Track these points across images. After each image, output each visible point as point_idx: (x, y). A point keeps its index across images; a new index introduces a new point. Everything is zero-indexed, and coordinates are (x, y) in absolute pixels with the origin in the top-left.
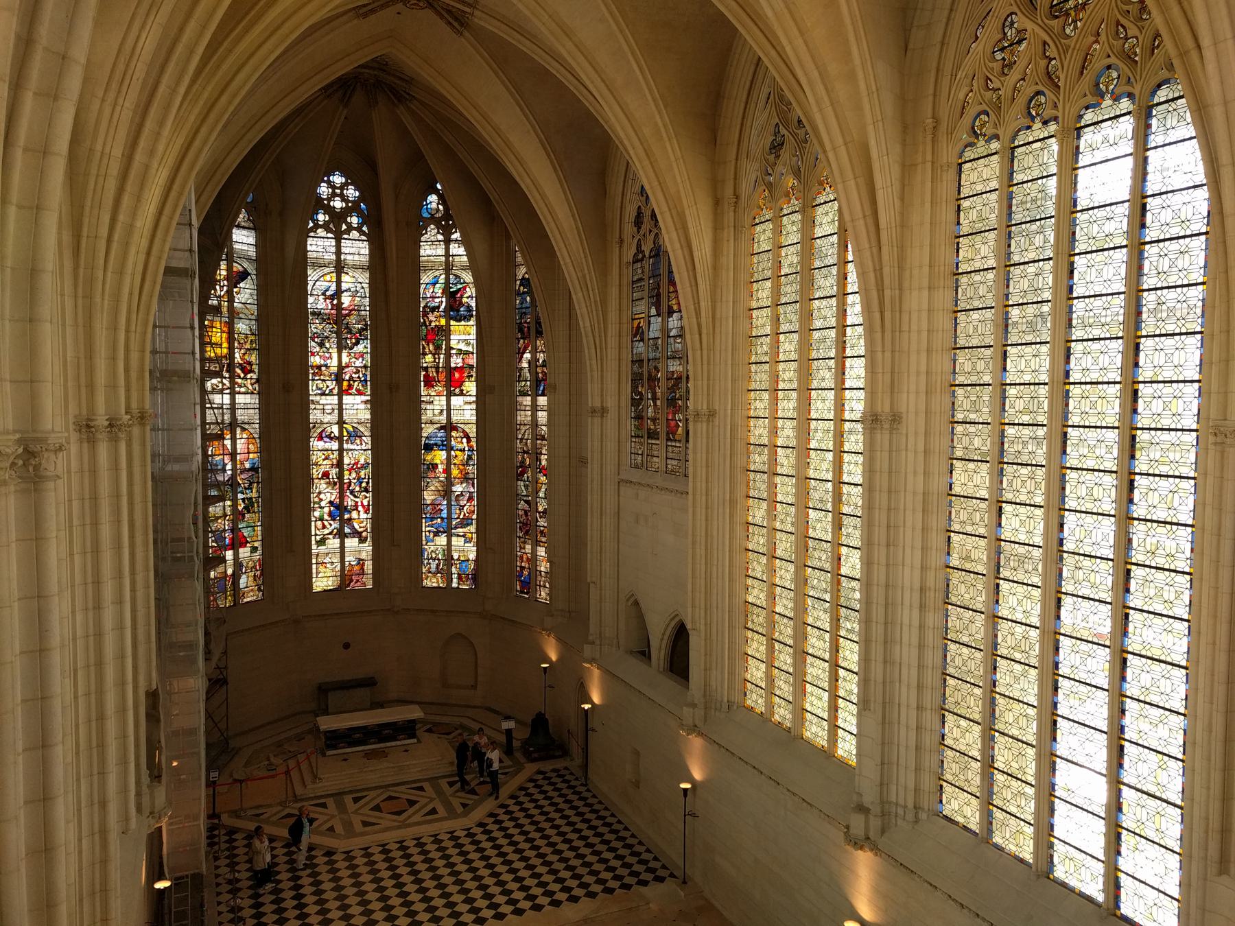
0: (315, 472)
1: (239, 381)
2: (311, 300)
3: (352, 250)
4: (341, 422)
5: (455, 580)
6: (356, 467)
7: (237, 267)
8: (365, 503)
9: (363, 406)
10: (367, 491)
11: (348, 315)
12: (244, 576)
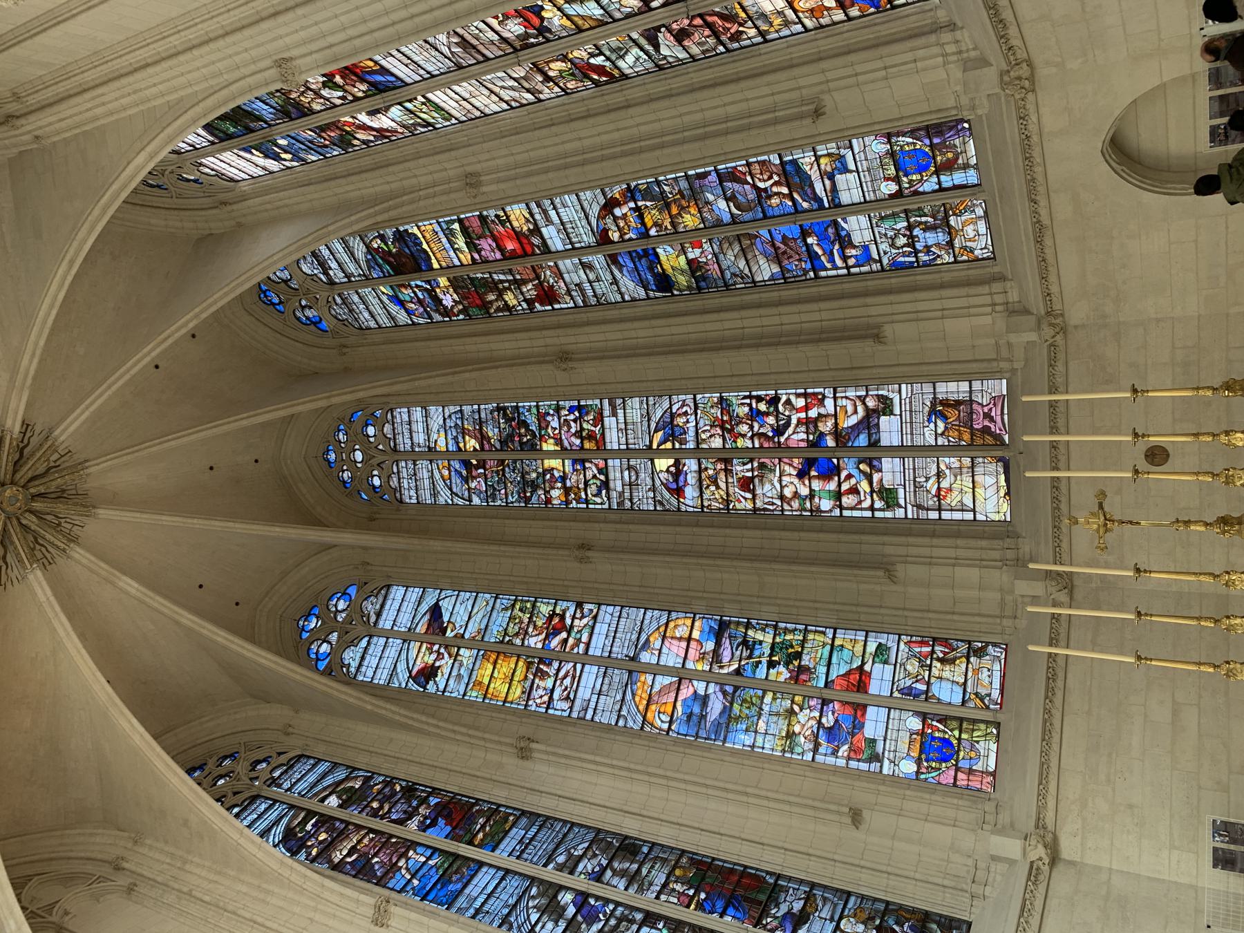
0: (744, 503)
1: (571, 641)
3: (407, 435)
4: (650, 453)
5: (959, 178)
6: (727, 426)
7: (421, 629)
8: (801, 403)
9: (620, 412)
10: (774, 401)
11: (489, 439)
12: (935, 690)
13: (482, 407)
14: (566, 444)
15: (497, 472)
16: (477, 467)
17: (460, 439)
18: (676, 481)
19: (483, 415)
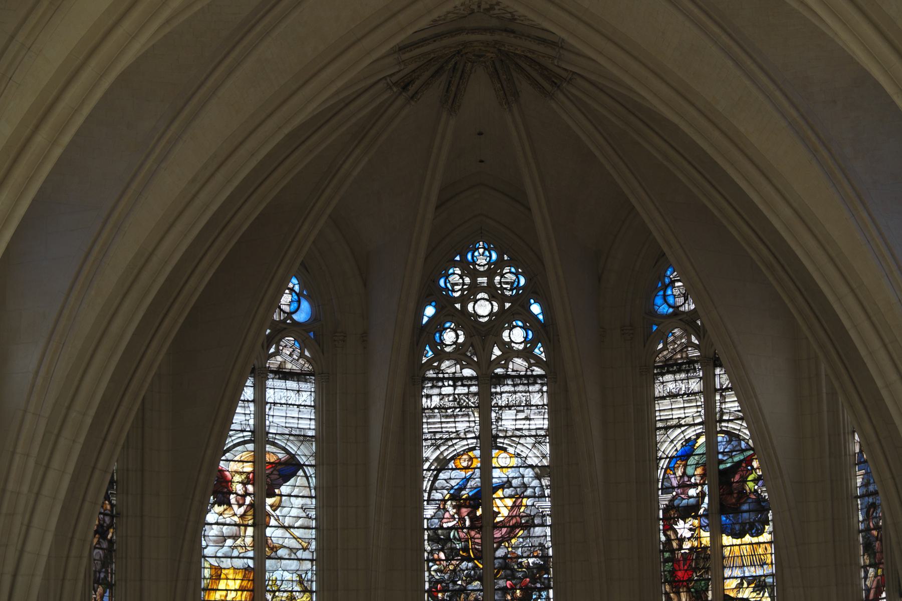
2: (429, 511)
3: (513, 399)
7: (273, 454)
11: (507, 538)
16: (473, 518)
17: (508, 491)
19: (538, 531)
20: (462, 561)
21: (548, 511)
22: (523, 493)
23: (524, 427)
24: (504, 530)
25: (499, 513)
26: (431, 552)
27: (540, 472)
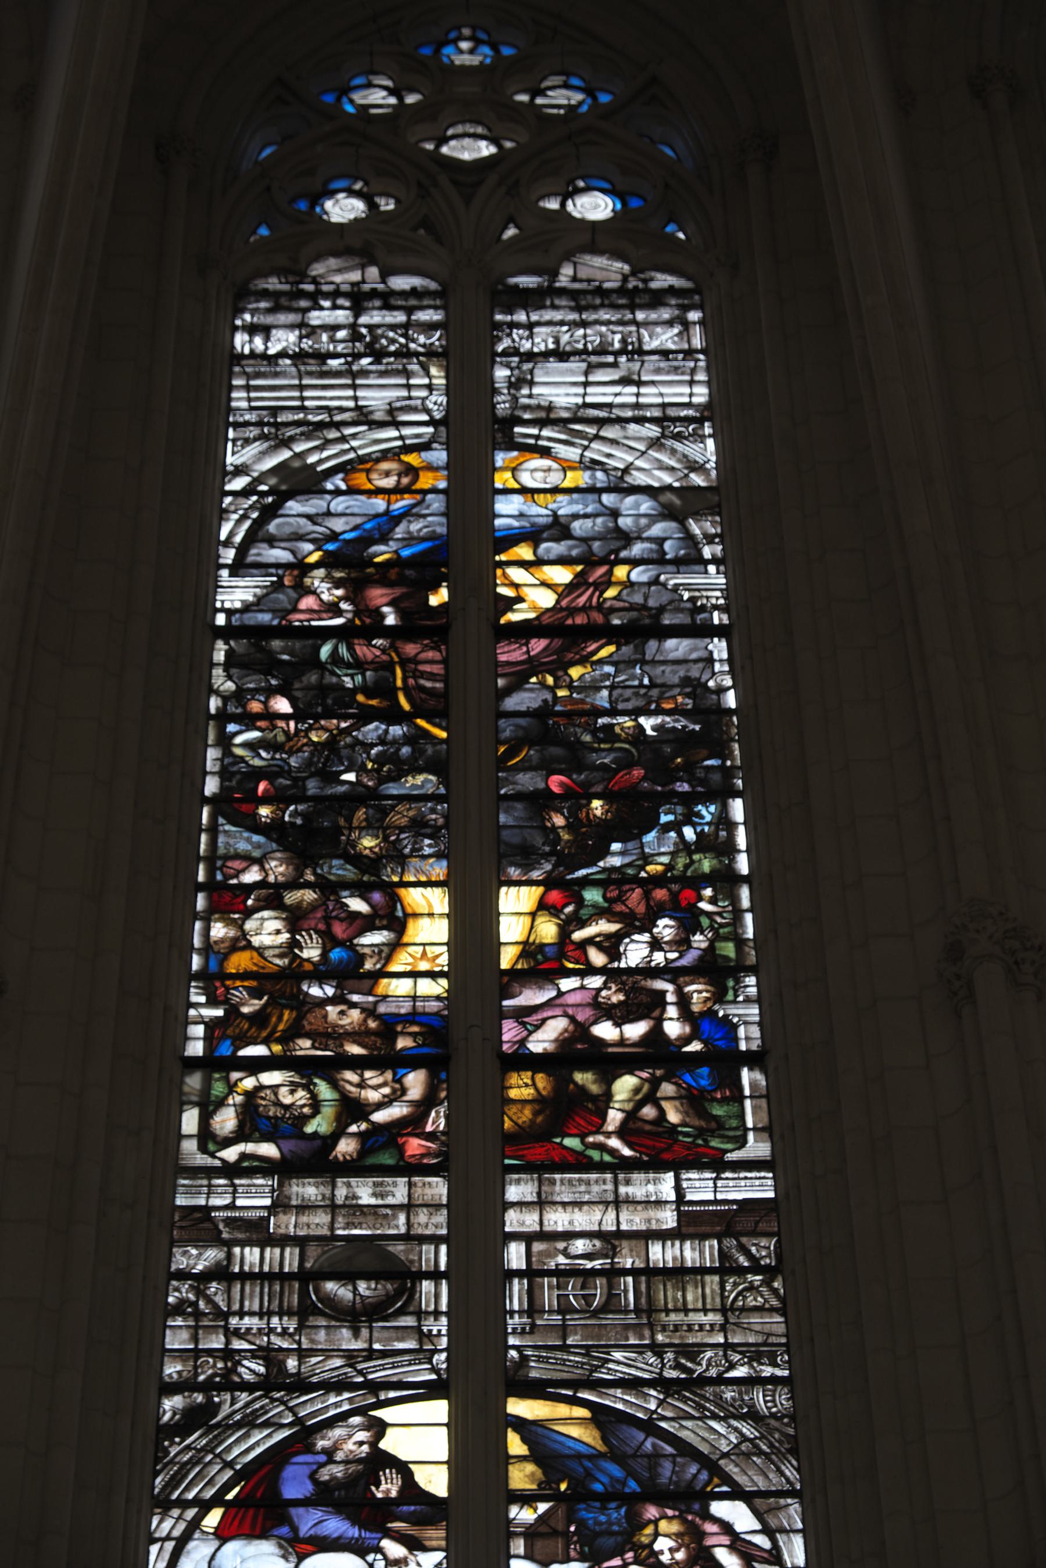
2: (235, 593)
13: (719, 648)
14: (531, 997)
15: (384, 689)
18: (325, 1496)
19: (676, 647)
20: (365, 716)
21: (716, 597)
22: (616, 552)
23: (619, 400)
24: (538, 645)
25: (520, 599)
26: (239, 696)
27: (678, 504)
